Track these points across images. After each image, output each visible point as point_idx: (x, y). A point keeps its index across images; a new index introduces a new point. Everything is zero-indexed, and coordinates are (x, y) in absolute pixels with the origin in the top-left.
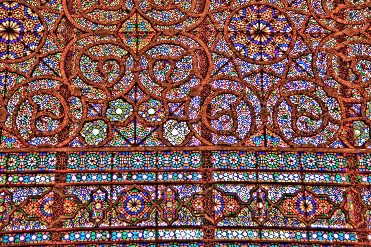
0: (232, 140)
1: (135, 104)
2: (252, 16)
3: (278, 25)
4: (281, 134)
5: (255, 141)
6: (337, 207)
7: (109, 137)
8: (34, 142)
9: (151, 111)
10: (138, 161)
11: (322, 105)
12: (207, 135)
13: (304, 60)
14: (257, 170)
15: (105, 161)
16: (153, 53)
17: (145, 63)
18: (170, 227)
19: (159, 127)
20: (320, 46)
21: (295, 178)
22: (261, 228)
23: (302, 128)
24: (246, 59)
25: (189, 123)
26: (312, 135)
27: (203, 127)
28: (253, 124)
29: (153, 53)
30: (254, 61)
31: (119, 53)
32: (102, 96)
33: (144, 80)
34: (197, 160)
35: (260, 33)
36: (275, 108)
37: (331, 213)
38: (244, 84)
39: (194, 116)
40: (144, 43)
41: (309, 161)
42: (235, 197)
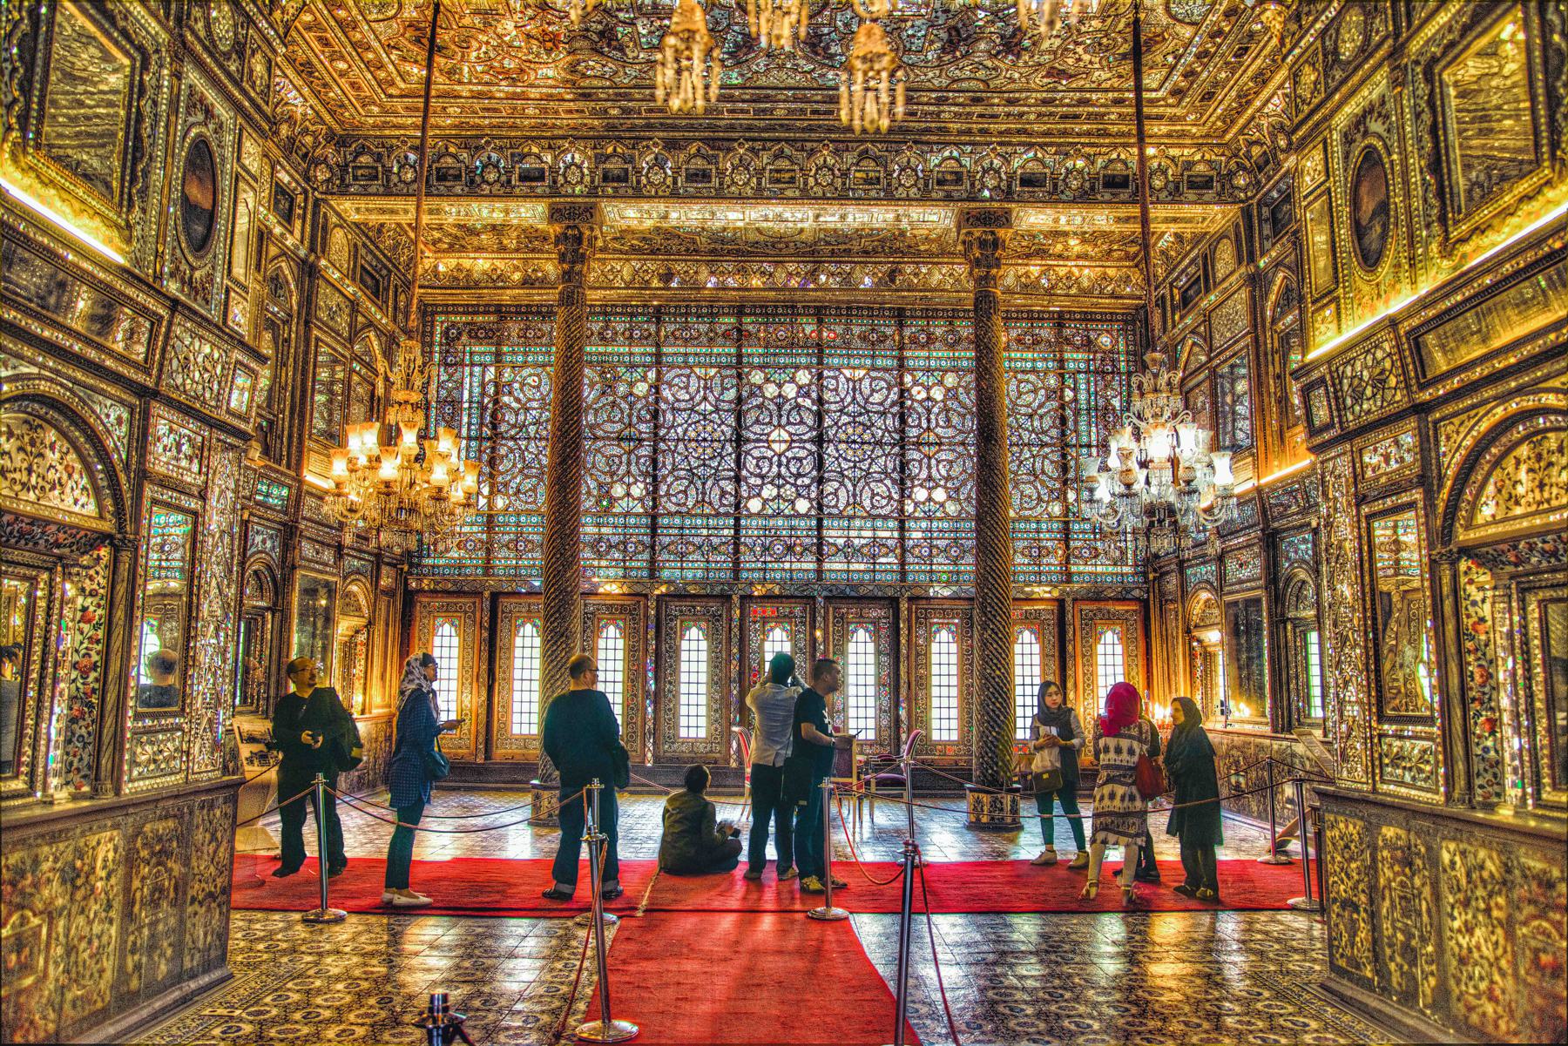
0: (835, 511)
1: (779, 487)
2: (850, 431)
3: (866, 437)
7: (764, 508)
8: (722, 510)
10: (780, 523)
12: (820, 507)
14: (849, 528)
15: (761, 522)
16: (789, 454)
17: (784, 460)
19: (793, 502)
21: (869, 534)
25: (811, 500)
29: (789, 454)
31: (770, 454)
32: (759, 482)
33: (783, 470)
34: (814, 523)
35: (854, 442)
39: (813, 495)
40: (784, 446)
41: (879, 523)
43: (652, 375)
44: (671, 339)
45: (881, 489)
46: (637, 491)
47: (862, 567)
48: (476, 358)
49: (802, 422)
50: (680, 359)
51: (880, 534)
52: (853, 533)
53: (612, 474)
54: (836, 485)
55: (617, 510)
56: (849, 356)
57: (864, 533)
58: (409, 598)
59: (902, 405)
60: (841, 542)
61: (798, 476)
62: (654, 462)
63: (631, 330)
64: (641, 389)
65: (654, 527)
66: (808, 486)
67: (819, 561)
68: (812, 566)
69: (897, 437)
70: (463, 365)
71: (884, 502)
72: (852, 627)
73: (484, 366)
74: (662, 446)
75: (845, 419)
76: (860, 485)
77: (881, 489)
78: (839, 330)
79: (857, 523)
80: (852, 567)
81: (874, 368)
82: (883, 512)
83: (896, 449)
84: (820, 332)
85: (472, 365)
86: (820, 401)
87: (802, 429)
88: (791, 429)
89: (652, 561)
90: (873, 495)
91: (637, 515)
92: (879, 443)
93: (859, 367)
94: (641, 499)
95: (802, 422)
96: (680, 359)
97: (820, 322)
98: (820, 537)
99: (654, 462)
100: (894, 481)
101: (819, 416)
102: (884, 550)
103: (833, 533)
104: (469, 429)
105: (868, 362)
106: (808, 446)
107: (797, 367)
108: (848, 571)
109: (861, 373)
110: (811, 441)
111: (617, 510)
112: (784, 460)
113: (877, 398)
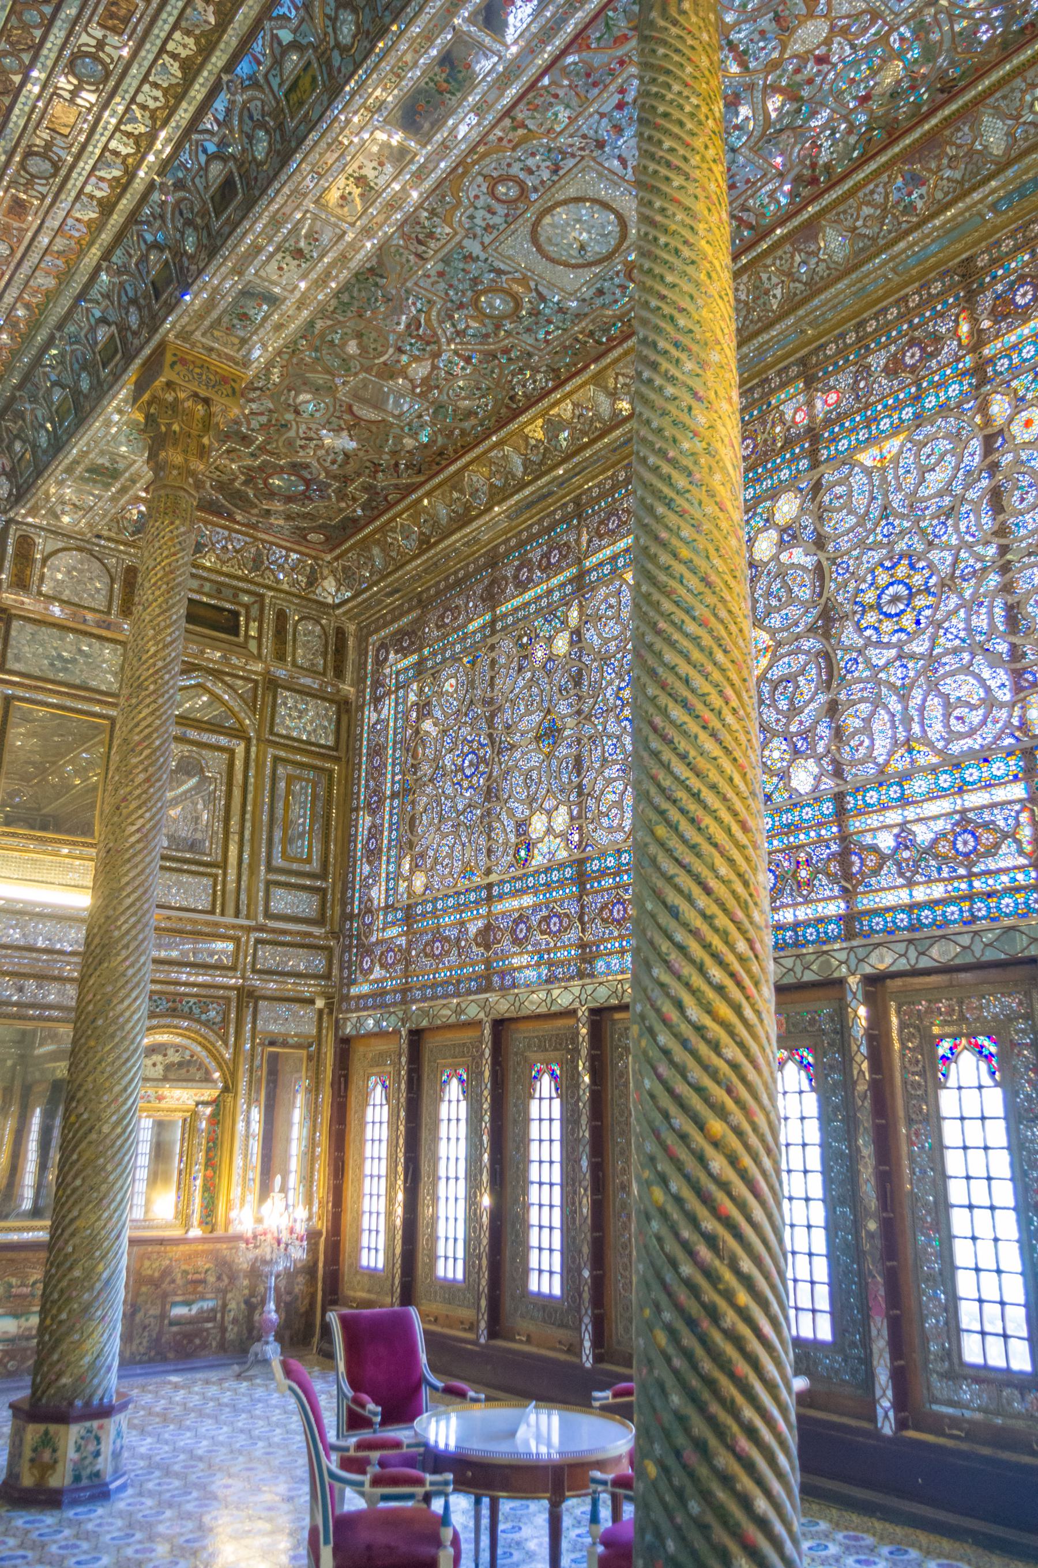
4: (930, 744)
5: (899, 764)
6: (1005, 836)
9: (776, 755)
11: (982, 682)
13: (954, 621)
18: (807, 901)
19: (784, 775)
20: (976, 592)
22: (910, 884)
23: (958, 727)
24: (879, 644)
25: (819, 759)
26: (971, 733)
27: (834, 761)
28: (894, 737)
29: (776, 673)
30: (888, 645)
34: (828, 808)
36: (922, 709)
37: (997, 846)
38: (878, 683)
39: (820, 749)
42: (874, 849)
43: (574, 614)
44: (596, 541)
45: (964, 688)
46: (561, 819)
47: (938, 891)
48: (401, 678)
49: (792, 600)
50: (607, 569)
51: (975, 799)
52: (911, 813)
53: (531, 800)
54: (864, 708)
55: (538, 860)
56: (868, 423)
57: (932, 808)
58: (345, 1046)
59: (993, 468)
60: (886, 841)
61: (794, 710)
62: (578, 761)
63: (546, 555)
64: (561, 644)
65: (581, 879)
66: (812, 729)
67: (848, 894)
68: (835, 908)
69: (992, 551)
70: (388, 693)
71: (976, 717)
72: (944, 1048)
73: (405, 686)
74: (588, 730)
75: (876, 556)
76: (917, 695)
77: (964, 688)
78: (844, 380)
79: (919, 786)
80: (920, 894)
81: (919, 419)
82: (975, 743)
83: (994, 580)
84: (810, 404)
85: (398, 689)
86: (820, 542)
87: (794, 611)
88: (775, 621)
89: (583, 945)
90: (948, 706)
91: (562, 866)
92: (949, 584)
93: (896, 430)
94: (563, 836)
95: (792, 600)
96: (607, 569)
97: (810, 382)
98: (844, 838)
99: (578, 761)
100: (995, 661)
101: (819, 571)
102: (987, 838)
103: (874, 821)
104: (393, 783)
105: (908, 413)
106: (807, 644)
107: (774, 495)
108: (911, 907)
109: (892, 446)
110: (811, 629)
111: (538, 860)
112: (766, 688)
113: (936, 479)
